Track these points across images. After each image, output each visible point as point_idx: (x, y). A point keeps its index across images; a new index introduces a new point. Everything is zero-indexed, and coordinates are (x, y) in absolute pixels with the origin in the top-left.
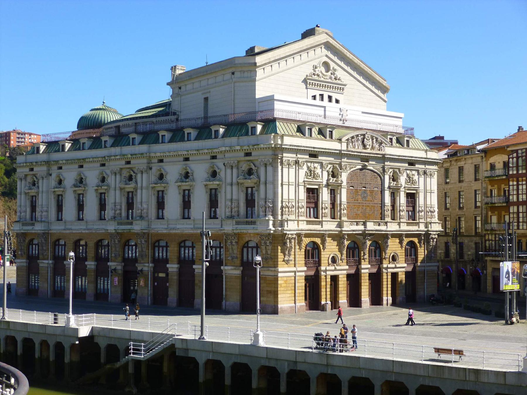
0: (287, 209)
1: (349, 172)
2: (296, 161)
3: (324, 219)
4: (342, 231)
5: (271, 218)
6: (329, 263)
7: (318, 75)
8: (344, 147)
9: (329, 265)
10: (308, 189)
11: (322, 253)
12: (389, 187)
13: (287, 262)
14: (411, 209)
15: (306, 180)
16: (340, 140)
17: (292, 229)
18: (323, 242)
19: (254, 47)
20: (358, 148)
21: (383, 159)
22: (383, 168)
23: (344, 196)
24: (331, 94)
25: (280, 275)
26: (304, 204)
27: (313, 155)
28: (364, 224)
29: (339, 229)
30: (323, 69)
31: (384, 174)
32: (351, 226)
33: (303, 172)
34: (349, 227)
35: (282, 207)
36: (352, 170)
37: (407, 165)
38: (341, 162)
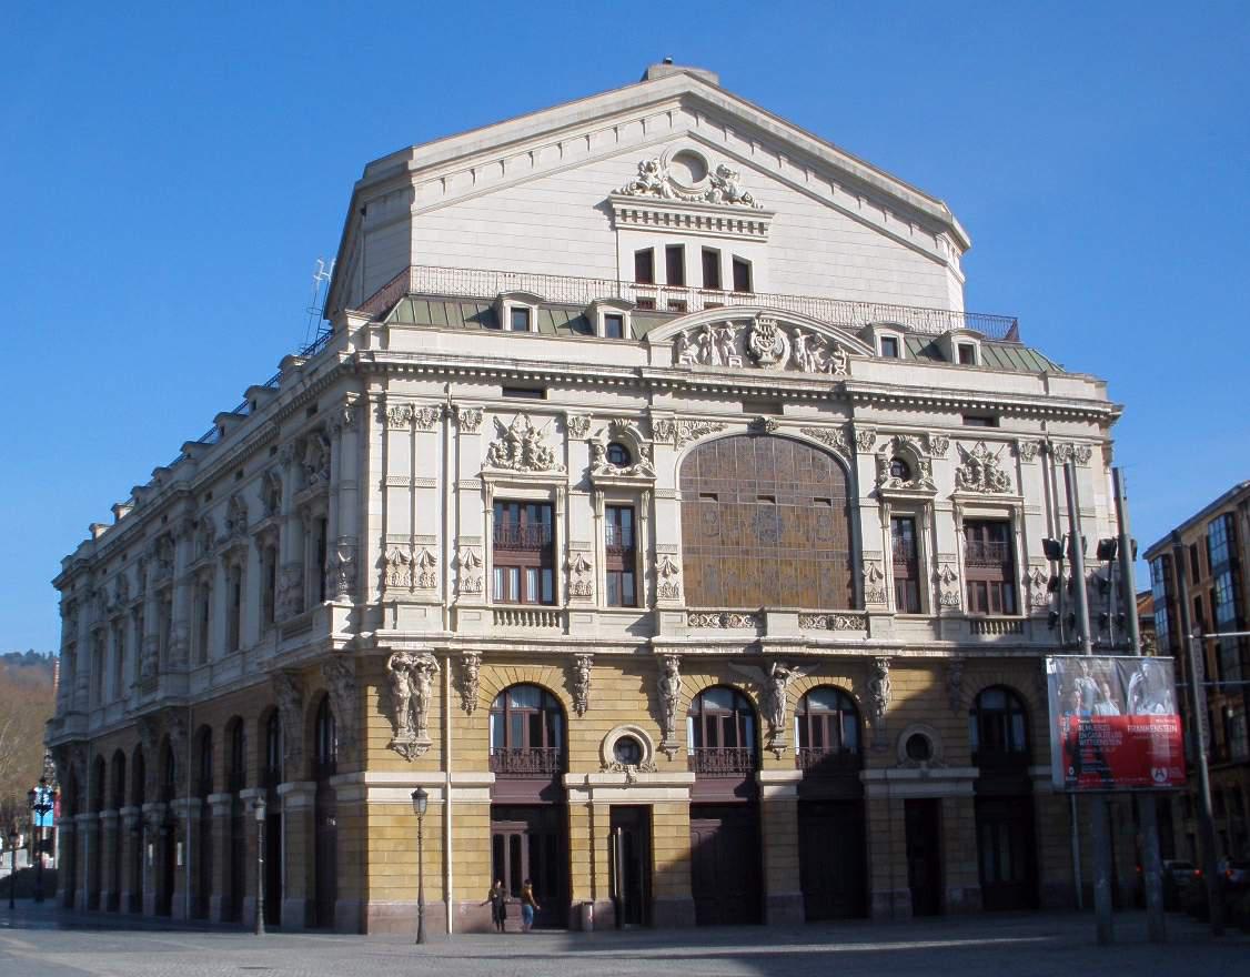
0: (404, 570)
1: (691, 445)
2: (444, 407)
3: (573, 604)
4: (649, 646)
5: (347, 601)
6: (602, 760)
7: (658, 190)
8: (662, 357)
9: (604, 766)
10: (496, 501)
11: (571, 725)
12: (877, 495)
13: (408, 752)
14: (995, 574)
15: (489, 469)
16: (644, 342)
17: (409, 632)
18: (574, 682)
19: (734, 256)
20: (726, 365)
21: (841, 398)
22: (848, 430)
23: (668, 526)
24: (713, 244)
25: (373, 795)
26: (485, 552)
27: (525, 386)
28: (760, 620)
29: (642, 640)
30: (683, 174)
31: (855, 454)
32: (695, 630)
33: (477, 446)
34: (675, 634)
35: (383, 563)
36: (703, 438)
37: (957, 419)
38: (647, 410)
